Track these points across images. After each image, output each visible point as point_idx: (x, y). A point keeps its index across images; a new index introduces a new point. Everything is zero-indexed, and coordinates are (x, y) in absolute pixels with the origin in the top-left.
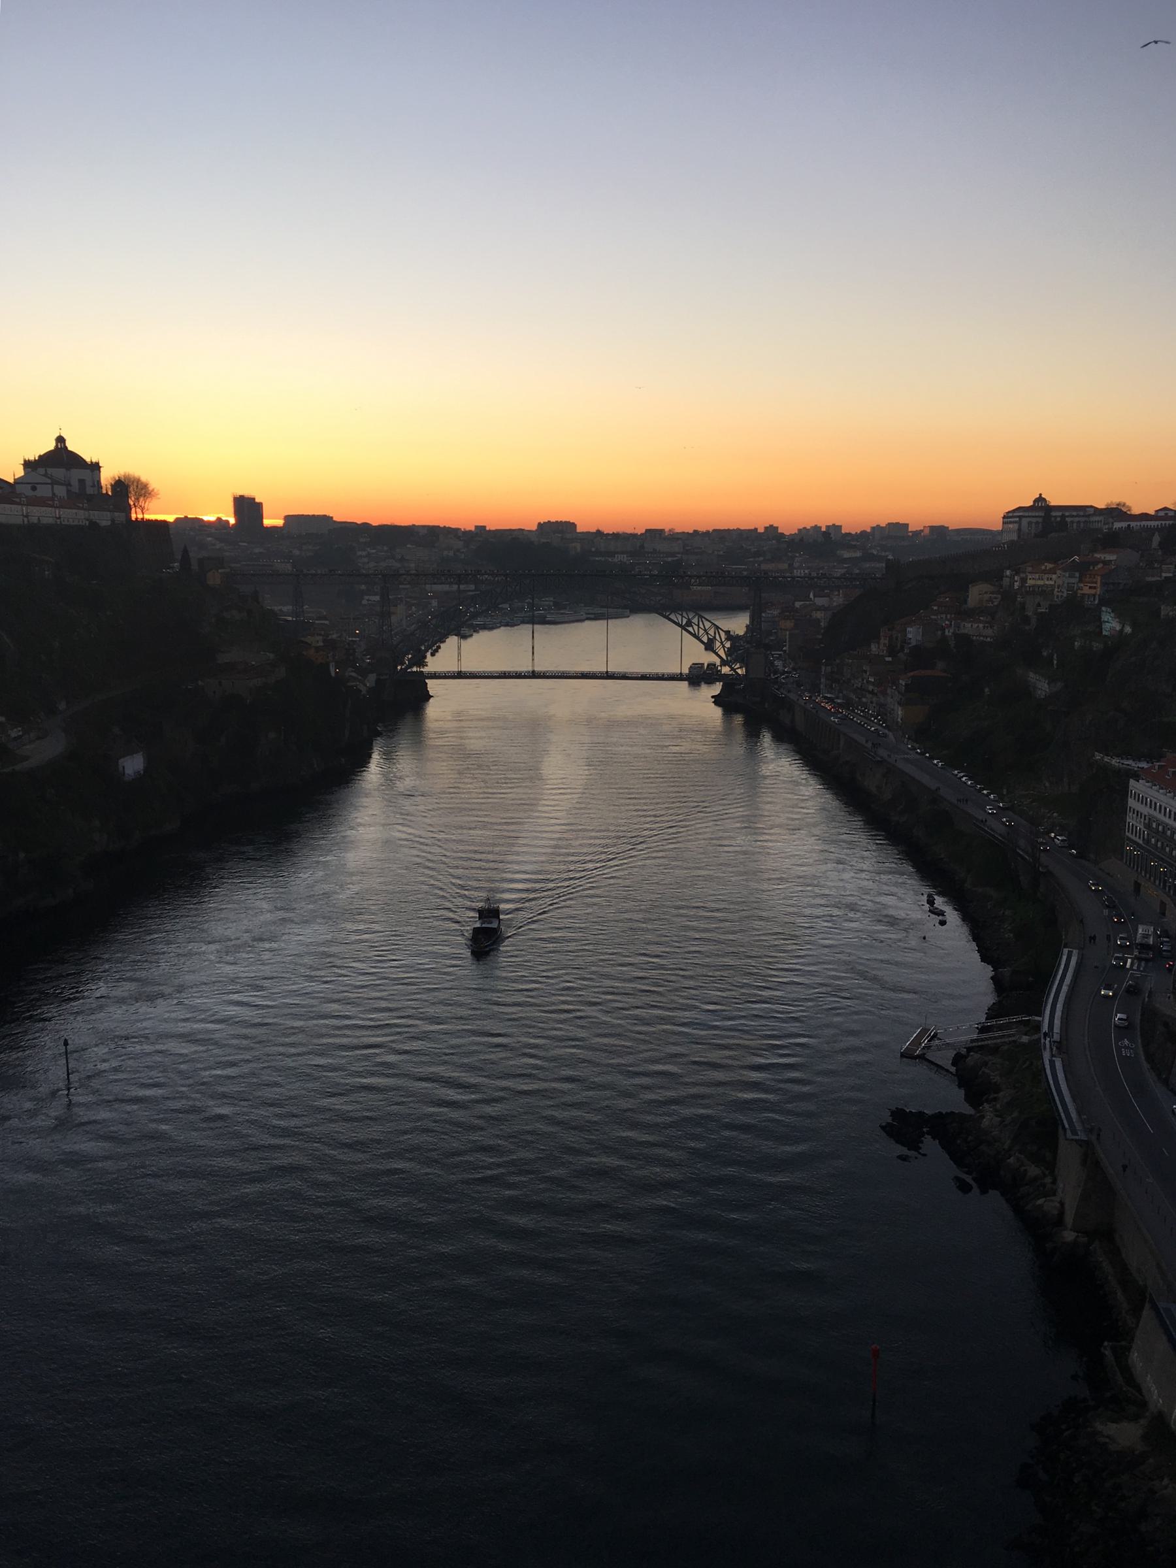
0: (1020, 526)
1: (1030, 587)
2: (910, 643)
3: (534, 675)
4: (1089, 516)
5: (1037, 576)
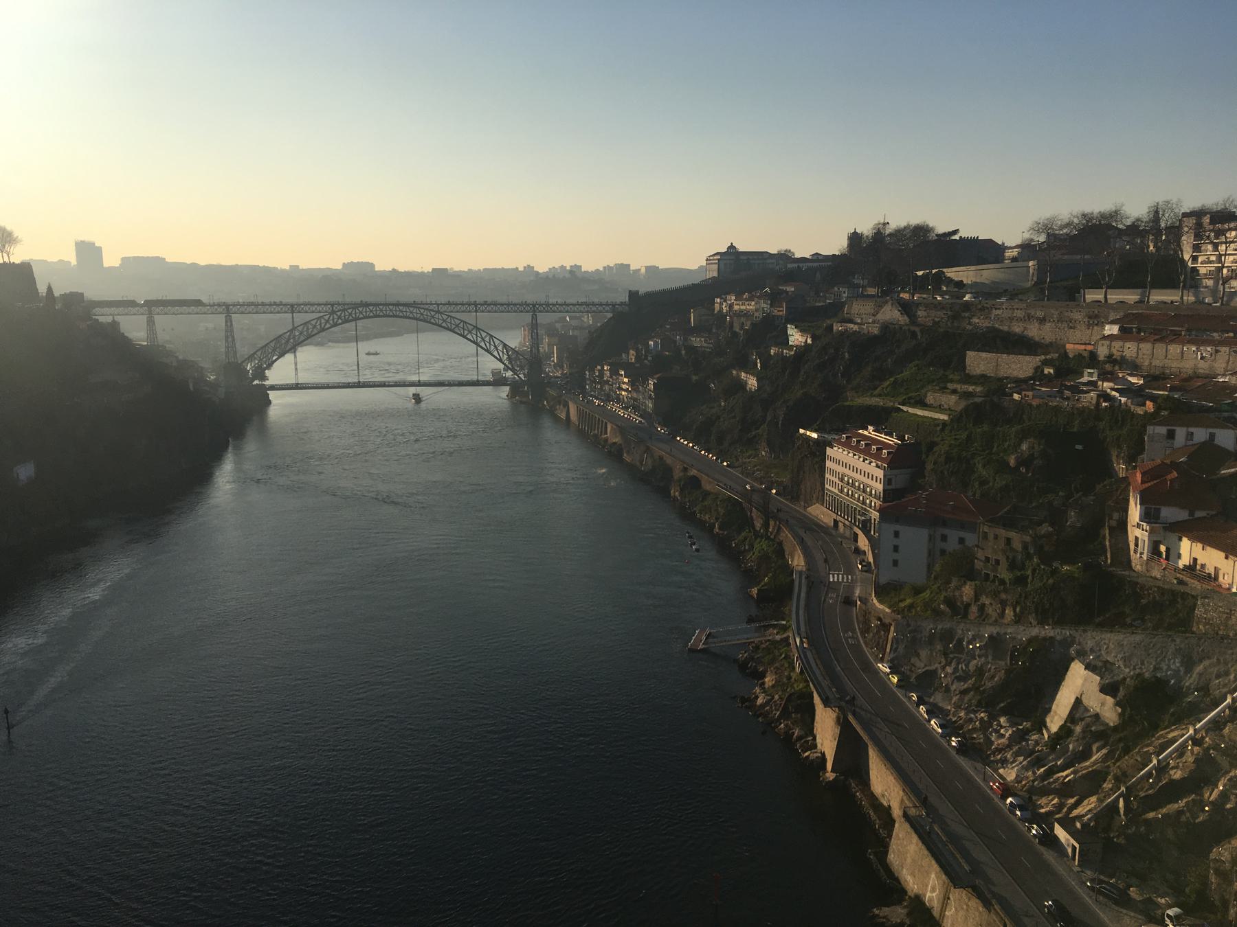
3: (359, 385)
4: (765, 259)
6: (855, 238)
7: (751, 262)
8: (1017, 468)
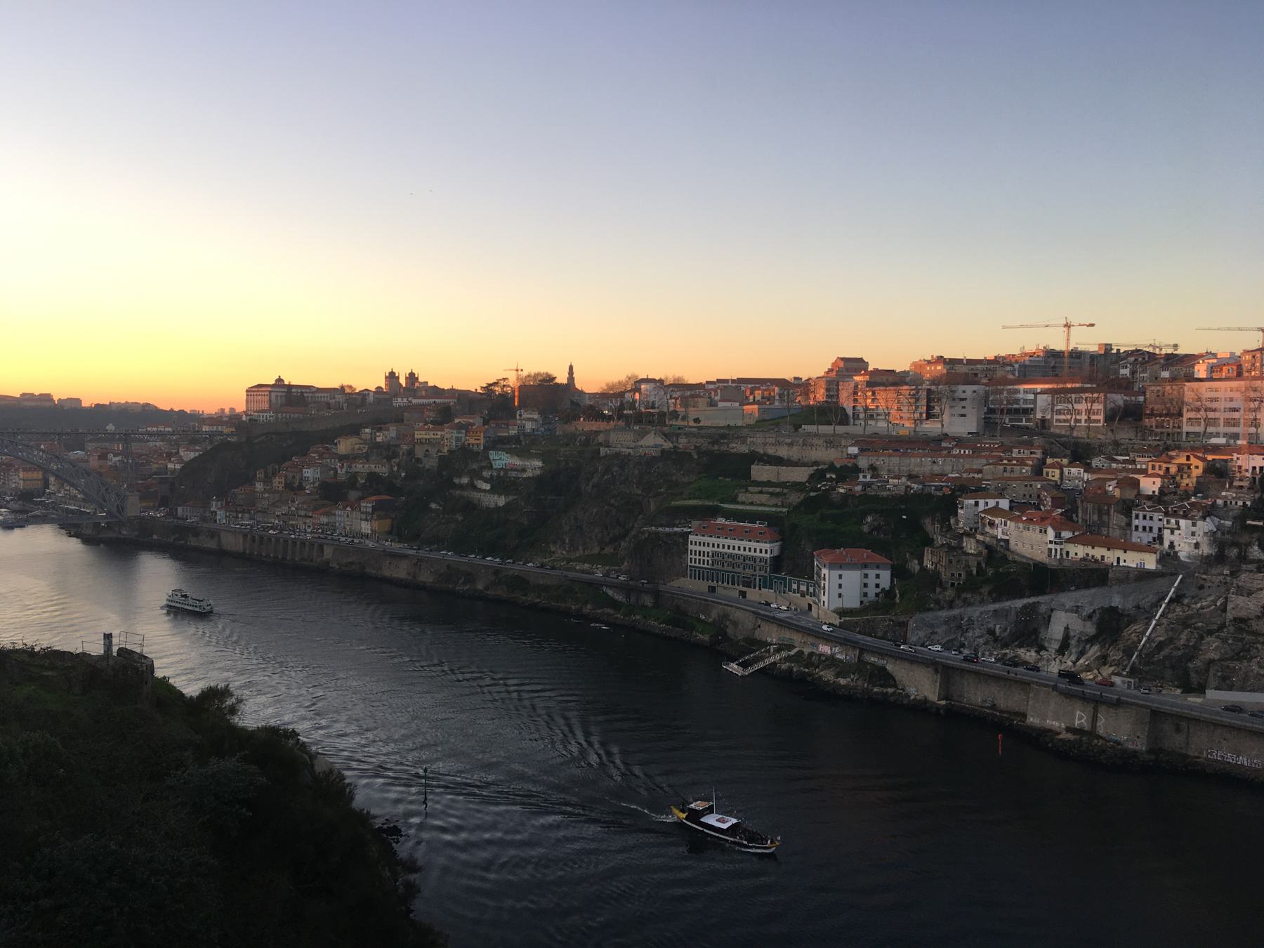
0: (270, 397)
4: (313, 392)
5: (424, 432)
6: (392, 377)
7: (306, 395)
8: (870, 533)
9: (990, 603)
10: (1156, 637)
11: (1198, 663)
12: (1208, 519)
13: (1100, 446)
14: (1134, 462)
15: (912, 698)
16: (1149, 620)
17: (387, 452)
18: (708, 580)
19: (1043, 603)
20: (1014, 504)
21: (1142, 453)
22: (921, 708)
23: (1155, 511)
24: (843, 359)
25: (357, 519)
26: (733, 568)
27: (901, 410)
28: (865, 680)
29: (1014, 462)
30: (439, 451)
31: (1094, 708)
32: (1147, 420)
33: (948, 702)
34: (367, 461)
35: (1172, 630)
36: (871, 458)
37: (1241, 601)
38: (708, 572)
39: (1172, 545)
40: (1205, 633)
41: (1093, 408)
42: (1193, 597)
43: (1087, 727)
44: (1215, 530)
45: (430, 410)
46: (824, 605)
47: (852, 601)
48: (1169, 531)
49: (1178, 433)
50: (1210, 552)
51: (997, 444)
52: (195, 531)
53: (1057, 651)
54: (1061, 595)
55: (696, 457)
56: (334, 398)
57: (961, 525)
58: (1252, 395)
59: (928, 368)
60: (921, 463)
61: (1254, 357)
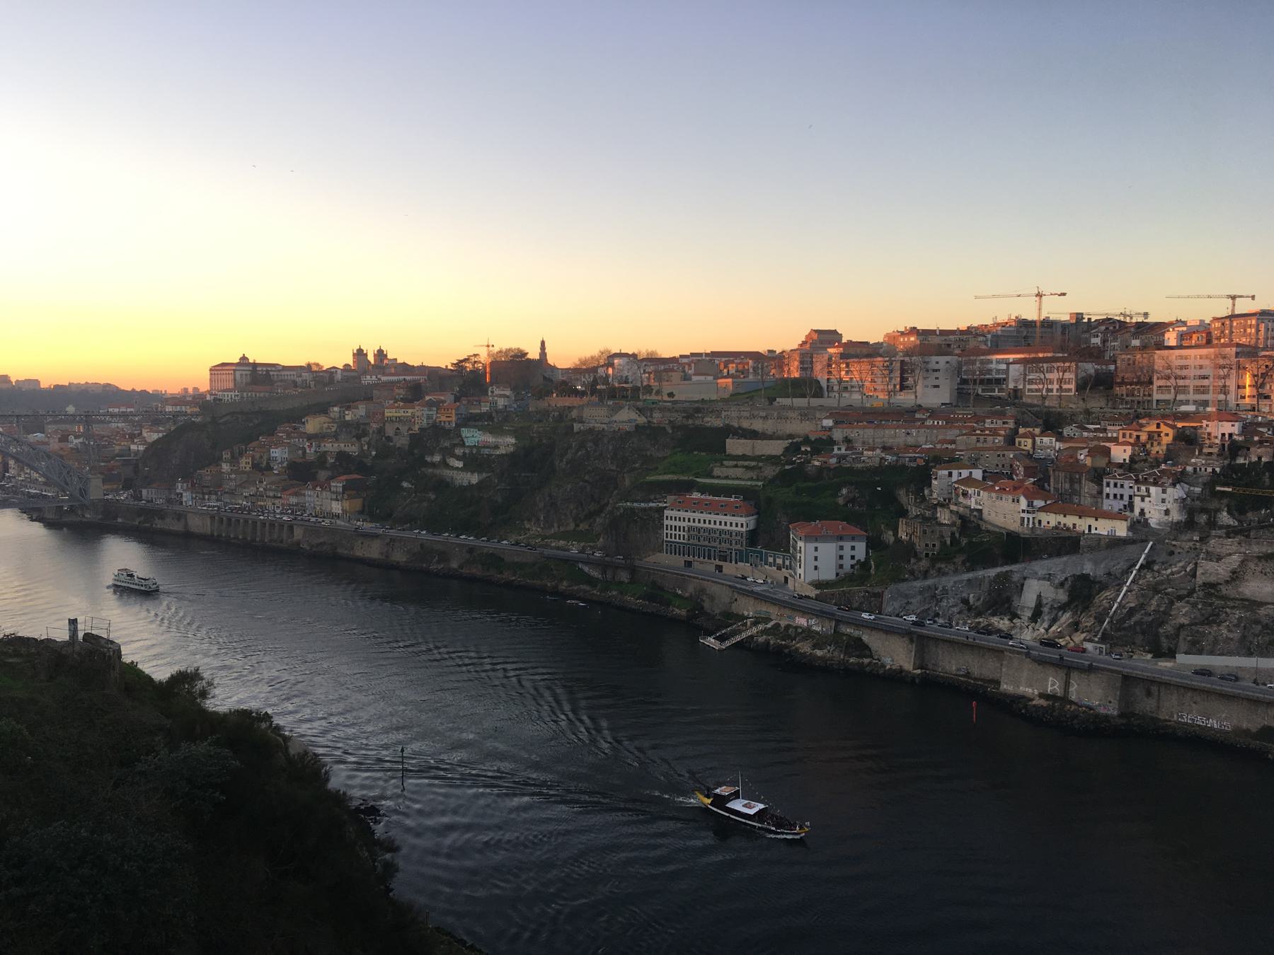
1: (388, 418)
2: (276, 460)
4: (279, 371)
6: (360, 354)
7: (271, 373)
8: (846, 505)
9: (964, 572)
10: (1127, 603)
11: (1168, 628)
12: (1178, 486)
13: (1071, 416)
14: (1105, 430)
15: (888, 667)
16: (1120, 586)
17: (357, 430)
18: (684, 555)
19: (1016, 572)
20: (986, 474)
21: (1113, 421)
22: (897, 677)
23: (1127, 479)
24: (816, 331)
25: (327, 499)
26: (709, 542)
27: (875, 382)
28: (841, 651)
29: (987, 432)
30: (410, 429)
31: (1066, 675)
32: (1118, 389)
33: (923, 671)
34: (337, 440)
35: (1143, 596)
36: (845, 430)
37: (1210, 566)
38: (684, 547)
39: (1142, 512)
40: (1175, 598)
41: (1065, 377)
42: (1163, 563)
43: (1060, 693)
44: (1185, 496)
45: (399, 388)
46: (800, 578)
47: (828, 574)
48: (1140, 498)
49: (1149, 401)
50: (1180, 518)
51: (970, 414)
52: (161, 514)
53: (1030, 618)
54: (1034, 563)
55: (671, 432)
56: (301, 376)
57: (935, 495)
58: (1221, 362)
59: (902, 340)
60: (896, 435)
61: (1223, 324)
